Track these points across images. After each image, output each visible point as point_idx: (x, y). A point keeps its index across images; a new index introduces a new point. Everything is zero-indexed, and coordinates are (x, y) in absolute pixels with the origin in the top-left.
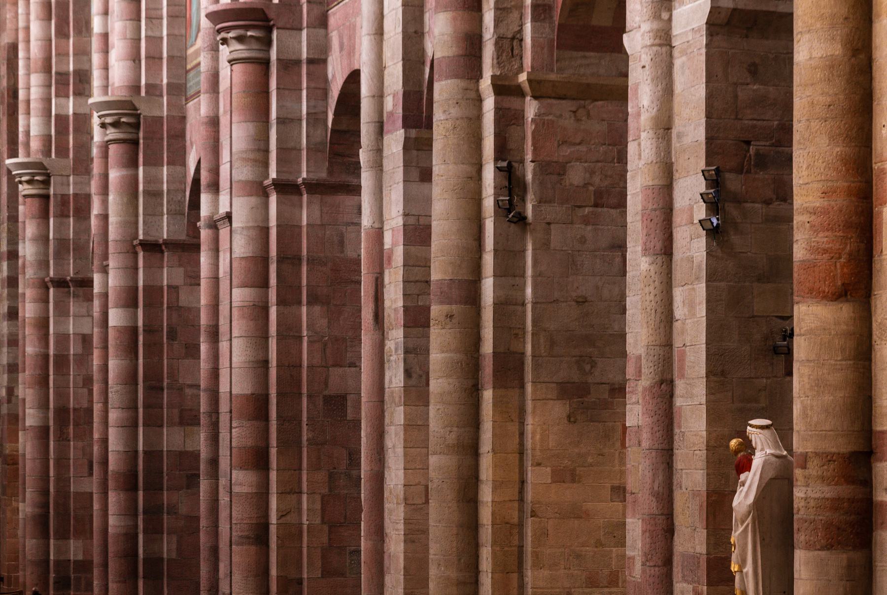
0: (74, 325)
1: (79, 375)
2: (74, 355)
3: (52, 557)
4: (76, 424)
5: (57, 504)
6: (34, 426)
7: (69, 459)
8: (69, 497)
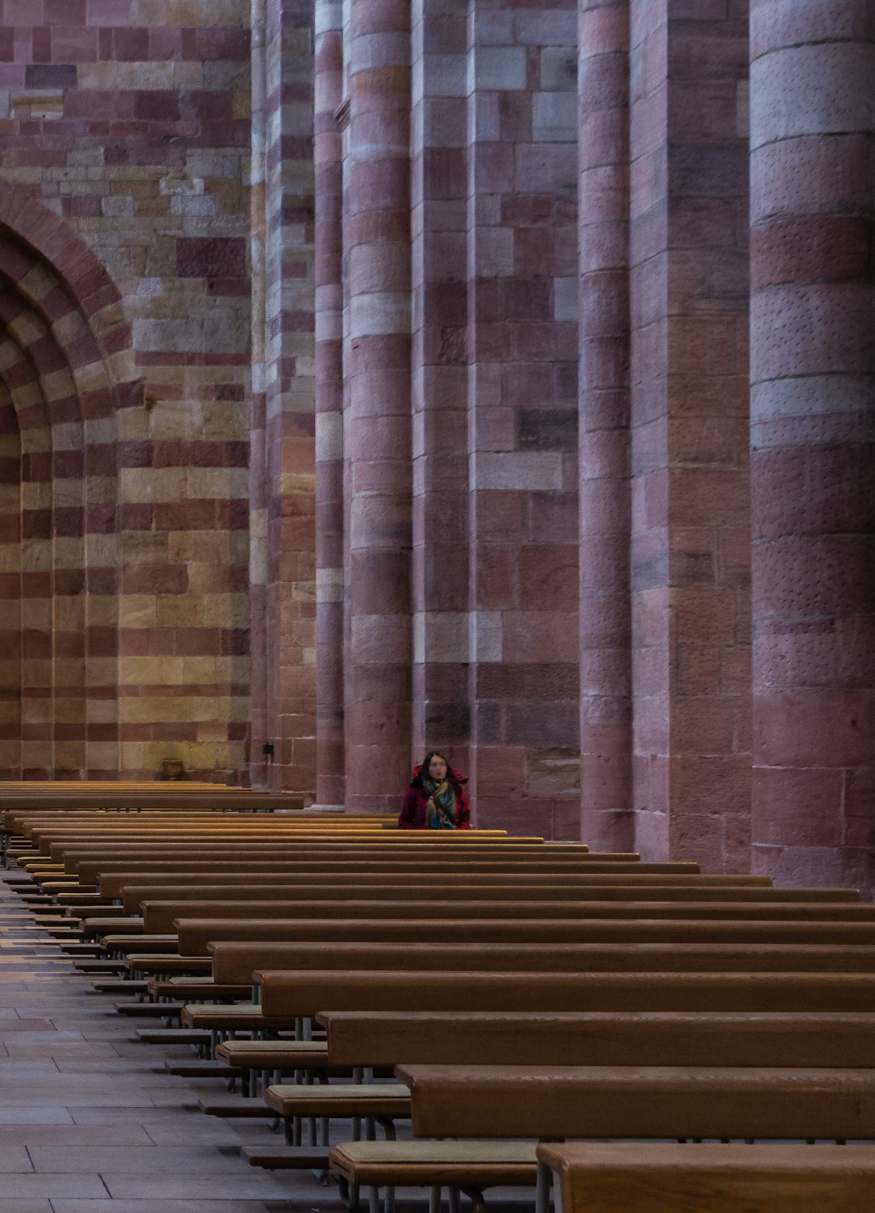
0: (478, 68)
1: (492, 194)
2: (478, 143)
3: (420, 657)
4: (485, 319)
5: (433, 523)
6: (377, 336)
7: (466, 410)
8: (466, 506)
